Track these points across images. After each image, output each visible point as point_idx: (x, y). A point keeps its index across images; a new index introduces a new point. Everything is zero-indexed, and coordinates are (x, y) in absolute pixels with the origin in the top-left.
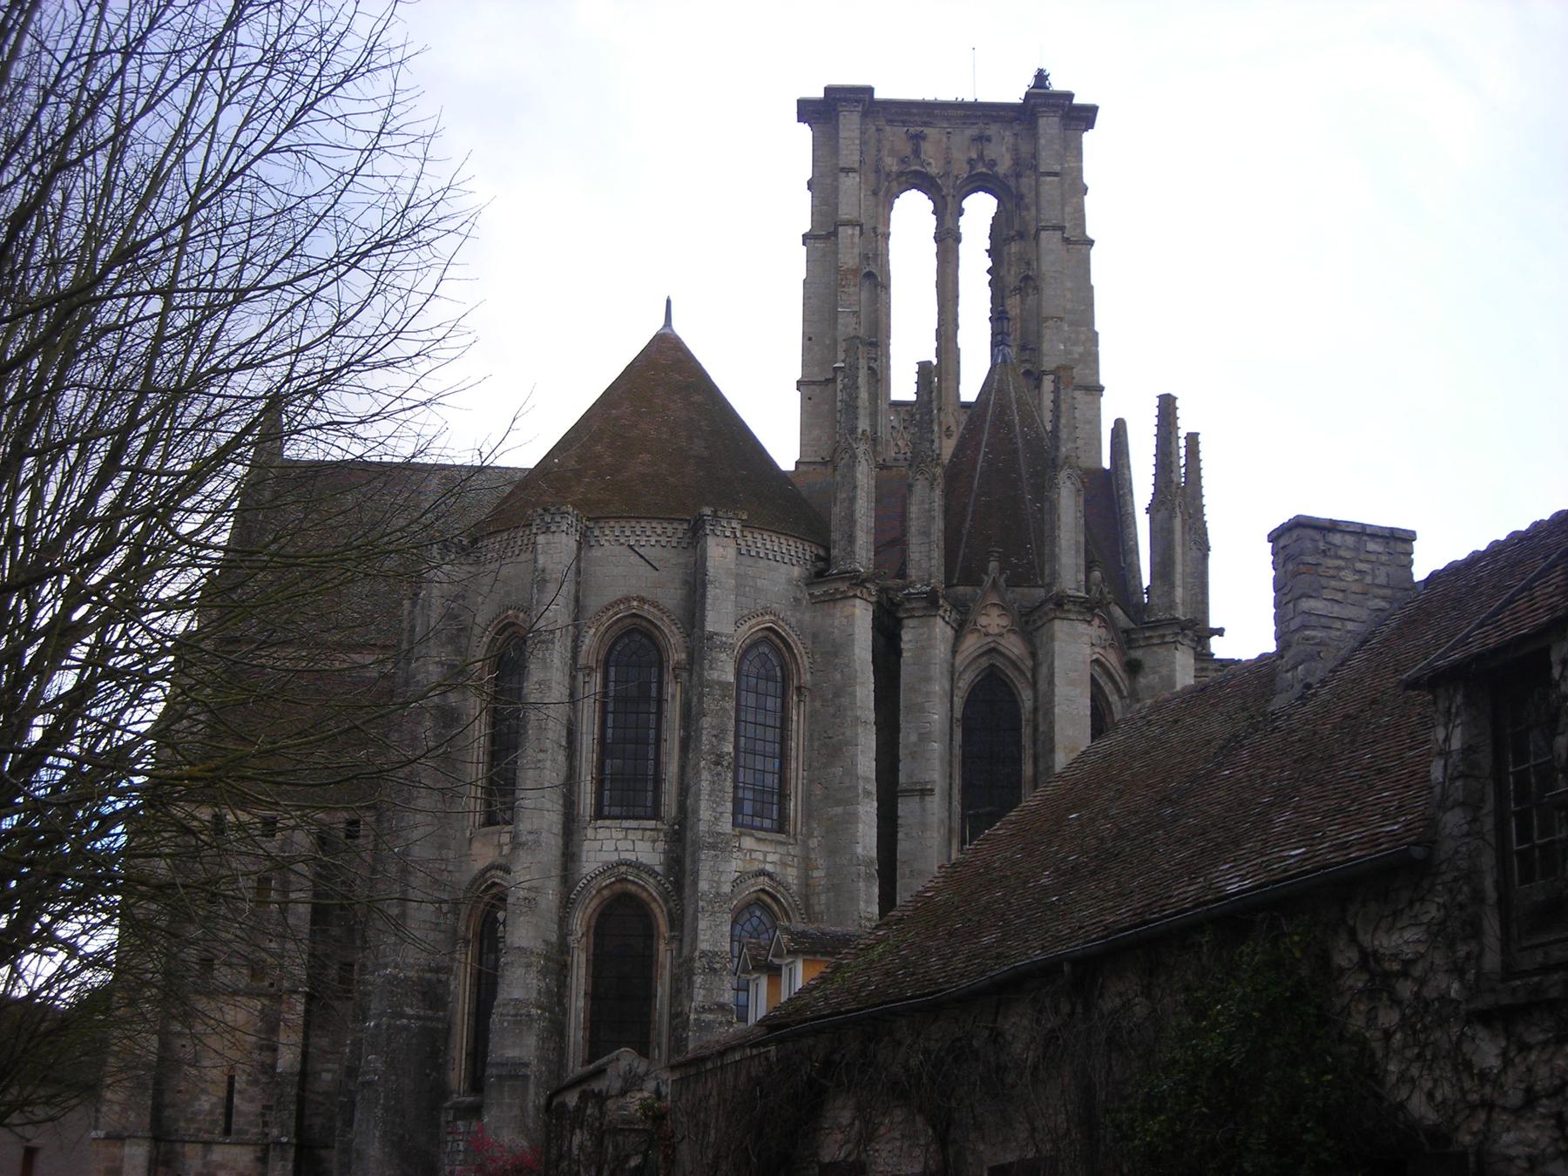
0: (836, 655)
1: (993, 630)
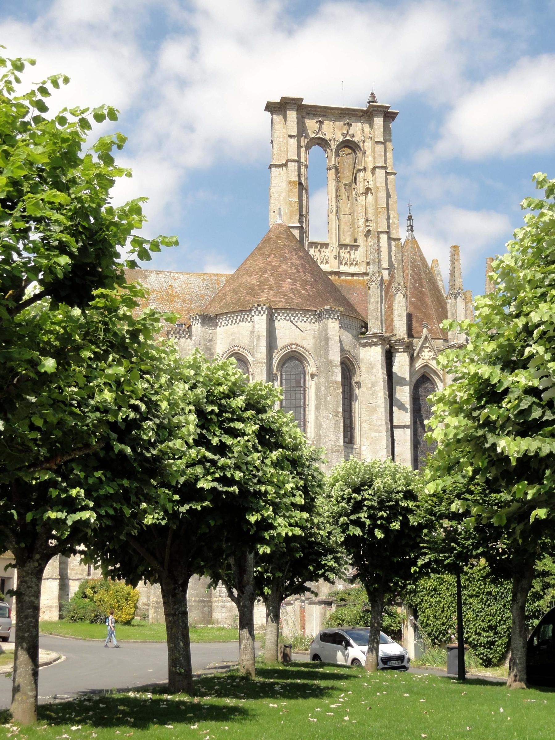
0: (372, 368)
1: (426, 357)
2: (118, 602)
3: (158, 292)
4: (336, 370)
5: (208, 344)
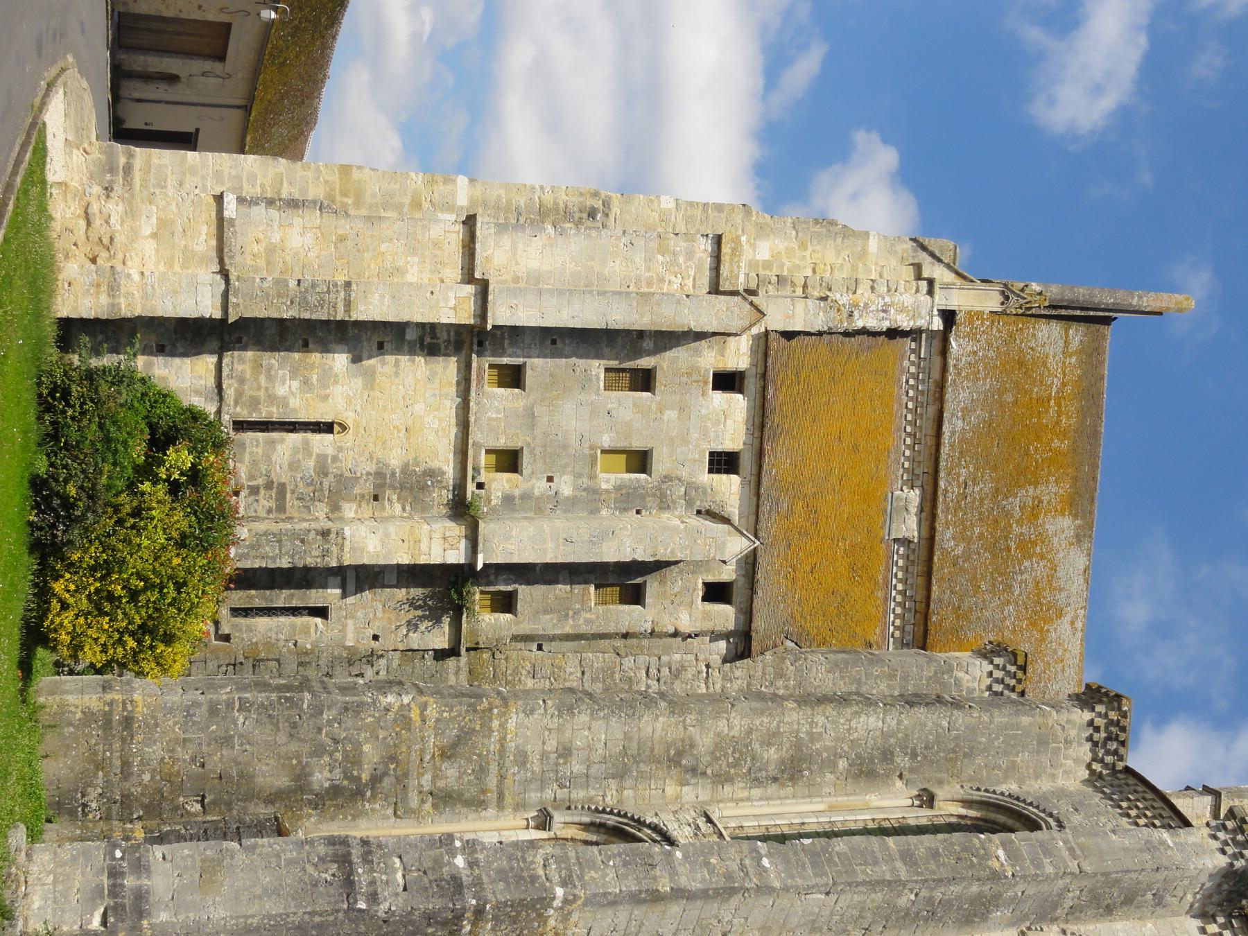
2: (134, 595)
3: (1051, 578)
5: (1149, 896)
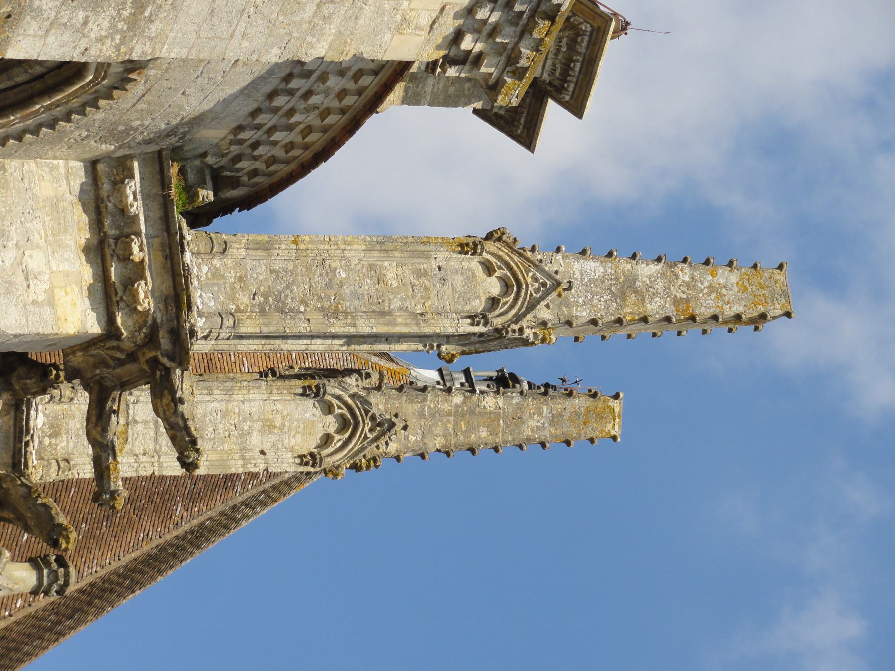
4: (100, 24)
